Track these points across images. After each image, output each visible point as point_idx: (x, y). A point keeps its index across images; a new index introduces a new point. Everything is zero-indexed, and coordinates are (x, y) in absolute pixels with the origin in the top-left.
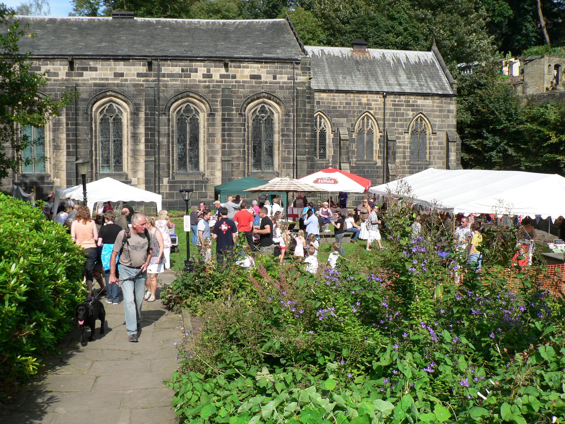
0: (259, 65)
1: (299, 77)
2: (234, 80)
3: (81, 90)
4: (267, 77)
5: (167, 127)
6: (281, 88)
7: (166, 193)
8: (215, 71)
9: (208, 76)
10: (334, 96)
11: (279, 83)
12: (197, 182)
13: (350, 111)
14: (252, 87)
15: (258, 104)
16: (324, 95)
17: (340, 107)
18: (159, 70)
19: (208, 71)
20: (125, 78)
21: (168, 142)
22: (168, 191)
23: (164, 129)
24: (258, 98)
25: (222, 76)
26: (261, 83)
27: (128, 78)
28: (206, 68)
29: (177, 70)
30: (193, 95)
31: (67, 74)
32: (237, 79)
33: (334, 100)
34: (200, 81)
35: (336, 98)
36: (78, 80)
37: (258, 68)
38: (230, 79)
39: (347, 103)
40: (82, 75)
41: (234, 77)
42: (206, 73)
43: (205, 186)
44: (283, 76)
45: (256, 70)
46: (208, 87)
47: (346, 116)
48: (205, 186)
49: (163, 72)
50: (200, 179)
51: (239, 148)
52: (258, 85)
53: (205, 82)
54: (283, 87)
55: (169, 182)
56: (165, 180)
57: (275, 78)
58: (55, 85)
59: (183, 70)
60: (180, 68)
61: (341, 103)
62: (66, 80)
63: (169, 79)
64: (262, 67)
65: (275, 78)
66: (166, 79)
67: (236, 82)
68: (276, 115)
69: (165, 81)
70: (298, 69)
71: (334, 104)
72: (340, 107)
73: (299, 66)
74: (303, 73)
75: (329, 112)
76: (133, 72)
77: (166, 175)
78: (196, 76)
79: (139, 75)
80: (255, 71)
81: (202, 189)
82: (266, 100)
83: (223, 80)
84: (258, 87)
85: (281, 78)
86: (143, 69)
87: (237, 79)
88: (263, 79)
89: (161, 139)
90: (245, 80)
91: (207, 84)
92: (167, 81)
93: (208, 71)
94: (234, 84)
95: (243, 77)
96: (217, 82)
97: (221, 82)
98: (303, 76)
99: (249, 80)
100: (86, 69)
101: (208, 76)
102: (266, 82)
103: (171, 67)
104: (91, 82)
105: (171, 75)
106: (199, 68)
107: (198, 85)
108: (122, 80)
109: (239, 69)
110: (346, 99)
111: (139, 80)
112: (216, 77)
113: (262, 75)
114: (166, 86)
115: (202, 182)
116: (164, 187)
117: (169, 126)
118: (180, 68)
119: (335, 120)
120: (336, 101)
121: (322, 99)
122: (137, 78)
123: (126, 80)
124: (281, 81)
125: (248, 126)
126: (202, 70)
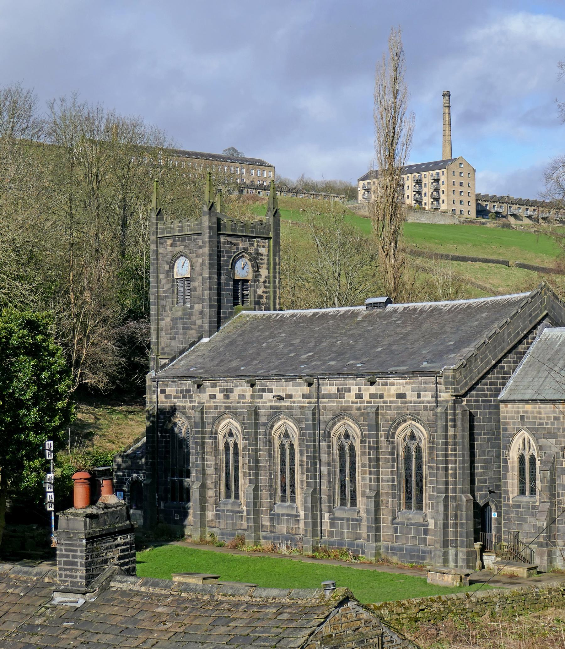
0: (404, 381)
1: (442, 394)
2: (382, 400)
3: (261, 414)
4: (411, 396)
5: (327, 455)
6: (425, 408)
7: (328, 531)
8: (365, 390)
9: (359, 396)
10: (540, 408)
11: (423, 403)
12: (353, 520)
13: (559, 429)
14: (398, 408)
15: (406, 428)
16: (529, 407)
17: (547, 424)
18: (319, 390)
19: (360, 390)
20: (293, 400)
21: (329, 472)
22: (329, 529)
23: (324, 457)
24: (405, 421)
25: (372, 396)
26: (406, 402)
27: (296, 400)
28: (357, 387)
29: (334, 390)
30: (348, 418)
31: (253, 397)
32: (385, 399)
33: (540, 413)
34: (353, 403)
35: (542, 410)
36: (259, 403)
37: (403, 384)
38: (378, 400)
39: (556, 418)
40: (261, 397)
41: (382, 396)
42: (357, 392)
43: (359, 524)
44: (427, 393)
45: (401, 386)
46: (359, 409)
47: (554, 436)
48: (360, 525)
49: (322, 393)
50: (356, 516)
51: (388, 481)
52: (403, 405)
53: (357, 403)
54: (427, 407)
55: (330, 519)
56: (327, 515)
57: (419, 396)
58: (243, 408)
59: (338, 391)
60: (337, 387)
61: (548, 418)
62: (251, 403)
63: (327, 400)
64: (407, 383)
65: (419, 396)
66: (325, 400)
67: (384, 402)
68: (423, 442)
69: (324, 403)
70: (441, 384)
71: (540, 419)
72: (547, 424)
73: (442, 380)
74: (446, 389)
75: (535, 430)
76: (299, 393)
77: (327, 510)
78: (349, 397)
79: (304, 396)
80: (400, 389)
81: (356, 529)
82: (413, 422)
83: (372, 400)
84: (404, 407)
85: (425, 396)
86: (306, 389)
87: (385, 399)
88: (408, 398)
89: (322, 468)
90: (391, 399)
91: (359, 405)
92: (326, 403)
93: (360, 391)
94: (382, 404)
95: (389, 396)
96: (367, 402)
97: (370, 402)
98: (446, 392)
99: (395, 399)
100: (264, 390)
101: (359, 396)
102: (411, 402)
103: (329, 387)
104: (269, 404)
105: (329, 396)
106: (351, 387)
107: (351, 407)
108: (291, 402)
109: (387, 387)
110: (554, 412)
111: (304, 402)
112: (366, 398)
113: (407, 393)
114: (325, 408)
115: (357, 520)
116: (325, 523)
117: (329, 453)
118: (337, 387)
119: (542, 441)
120: (542, 415)
121: (526, 412)
122: (303, 400)
123: (294, 402)
124: (425, 399)
125: (398, 455)
126: (355, 390)
